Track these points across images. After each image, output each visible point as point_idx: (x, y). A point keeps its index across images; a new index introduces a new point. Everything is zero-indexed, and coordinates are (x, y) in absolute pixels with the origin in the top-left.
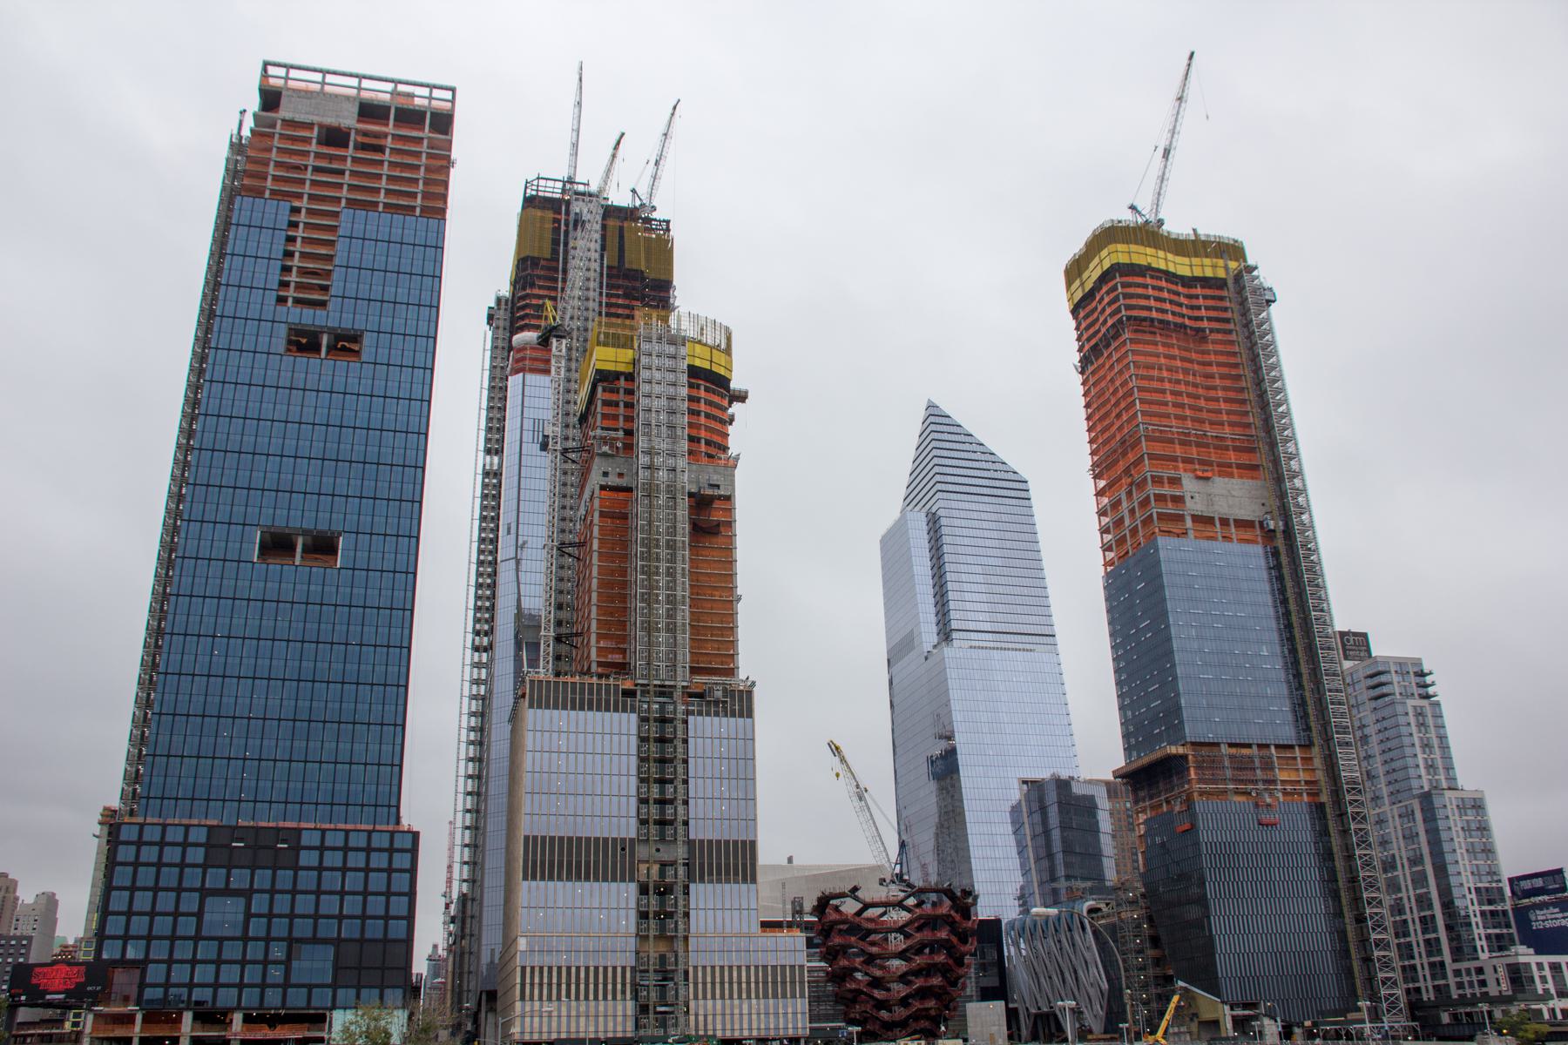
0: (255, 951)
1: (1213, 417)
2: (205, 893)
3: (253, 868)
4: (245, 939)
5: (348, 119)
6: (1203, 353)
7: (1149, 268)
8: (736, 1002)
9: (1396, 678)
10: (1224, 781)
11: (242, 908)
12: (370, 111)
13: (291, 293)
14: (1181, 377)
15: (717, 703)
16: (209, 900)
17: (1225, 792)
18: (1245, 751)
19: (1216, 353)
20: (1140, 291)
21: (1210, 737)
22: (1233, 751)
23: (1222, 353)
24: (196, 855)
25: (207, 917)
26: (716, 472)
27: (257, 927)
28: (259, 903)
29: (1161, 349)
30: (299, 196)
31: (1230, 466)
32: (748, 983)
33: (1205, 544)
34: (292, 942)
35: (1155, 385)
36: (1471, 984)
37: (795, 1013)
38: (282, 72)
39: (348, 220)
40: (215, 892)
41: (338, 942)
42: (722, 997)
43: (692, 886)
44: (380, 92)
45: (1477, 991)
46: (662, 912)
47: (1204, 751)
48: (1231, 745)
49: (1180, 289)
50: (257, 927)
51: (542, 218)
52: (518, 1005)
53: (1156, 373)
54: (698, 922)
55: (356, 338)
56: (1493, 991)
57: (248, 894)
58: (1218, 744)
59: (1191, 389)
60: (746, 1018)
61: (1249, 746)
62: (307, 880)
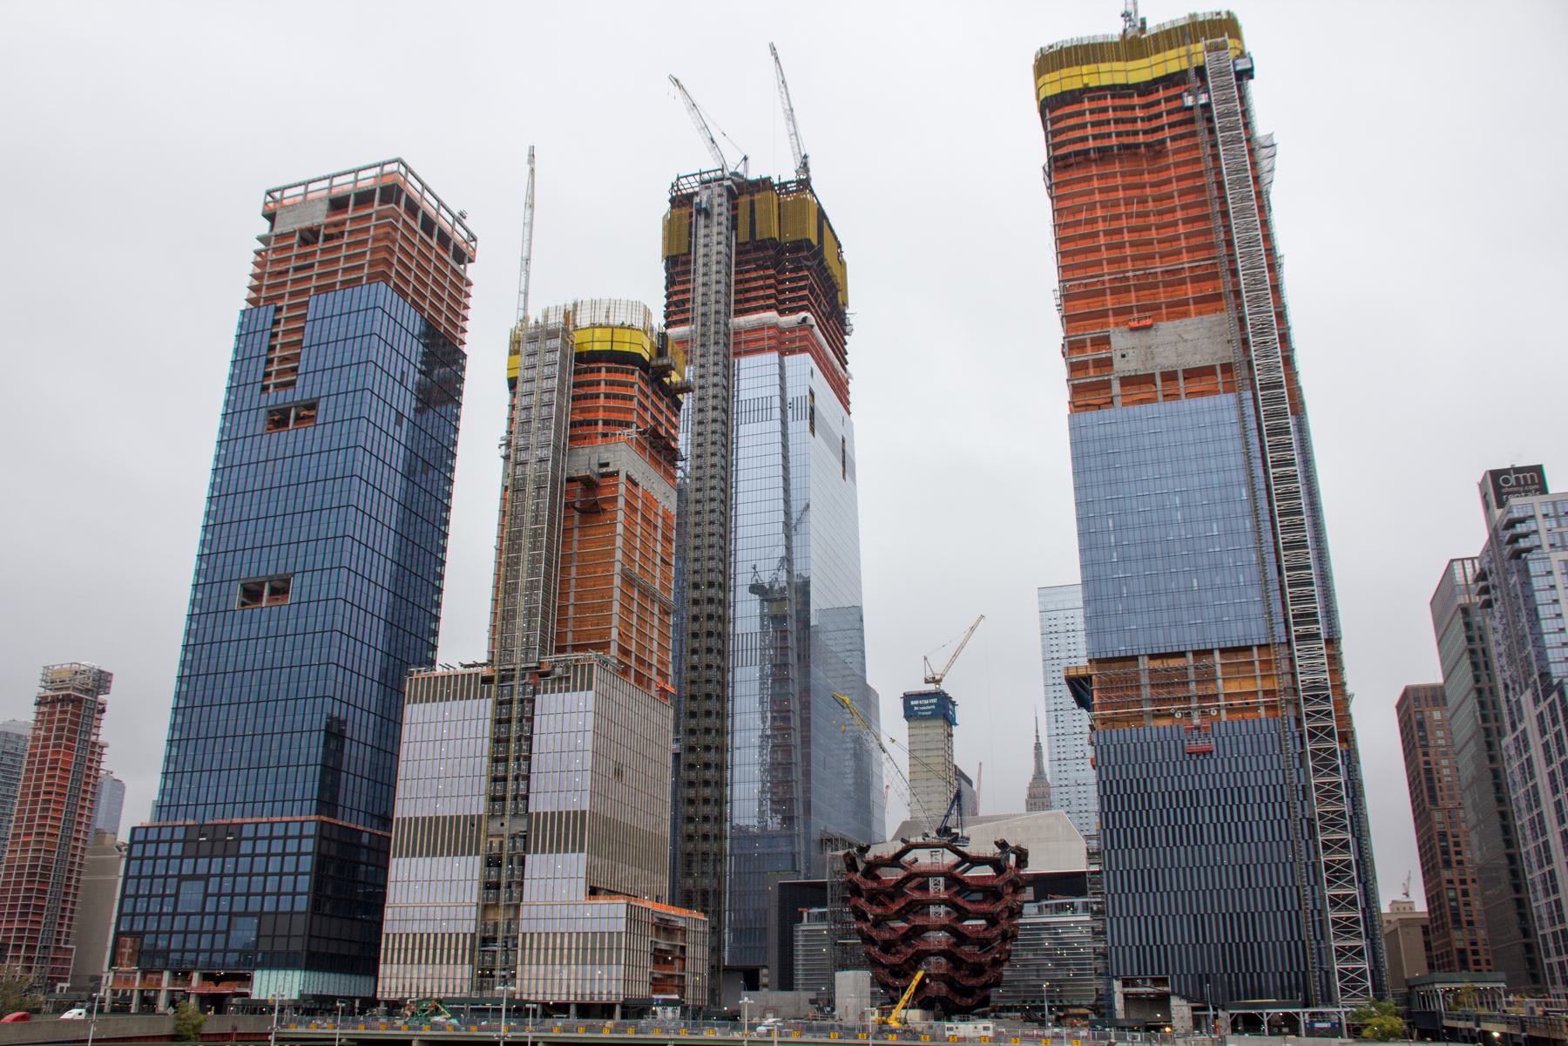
1: (1167, 247)
2: (181, 878)
3: (211, 857)
4: (203, 913)
5: (319, 216)
6: (1159, 170)
7: (1086, 90)
8: (557, 967)
9: (1543, 525)
10: (1139, 703)
12: (338, 204)
13: (273, 380)
14: (1123, 209)
15: (560, 679)
17: (1140, 716)
18: (1173, 663)
19: (1177, 165)
20: (1071, 122)
21: (1123, 650)
22: (1157, 664)
23: (1186, 163)
24: (177, 849)
26: (607, 451)
27: (210, 907)
28: (213, 886)
29: (1096, 184)
30: (282, 297)
31: (1186, 303)
32: (570, 949)
33: (1137, 410)
35: (1082, 230)
37: (609, 980)
39: (317, 305)
41: (261, 914)
42: (546, 963)
43: (528, 858)
44: (344, 185)
46: (501, 884)
47: (1115, 670)
48: (1152, 657)
49: (1136, 100)
51: (680, 217)
52: (381, 967)
53: (1083, 216)
54: (531, 890)
55: (312, 406)
57: (206, 878)
58: (1135, 658)
59: (1134, 222)
60: (565, 983)
61: (1182, 654)
62: (244, 864)
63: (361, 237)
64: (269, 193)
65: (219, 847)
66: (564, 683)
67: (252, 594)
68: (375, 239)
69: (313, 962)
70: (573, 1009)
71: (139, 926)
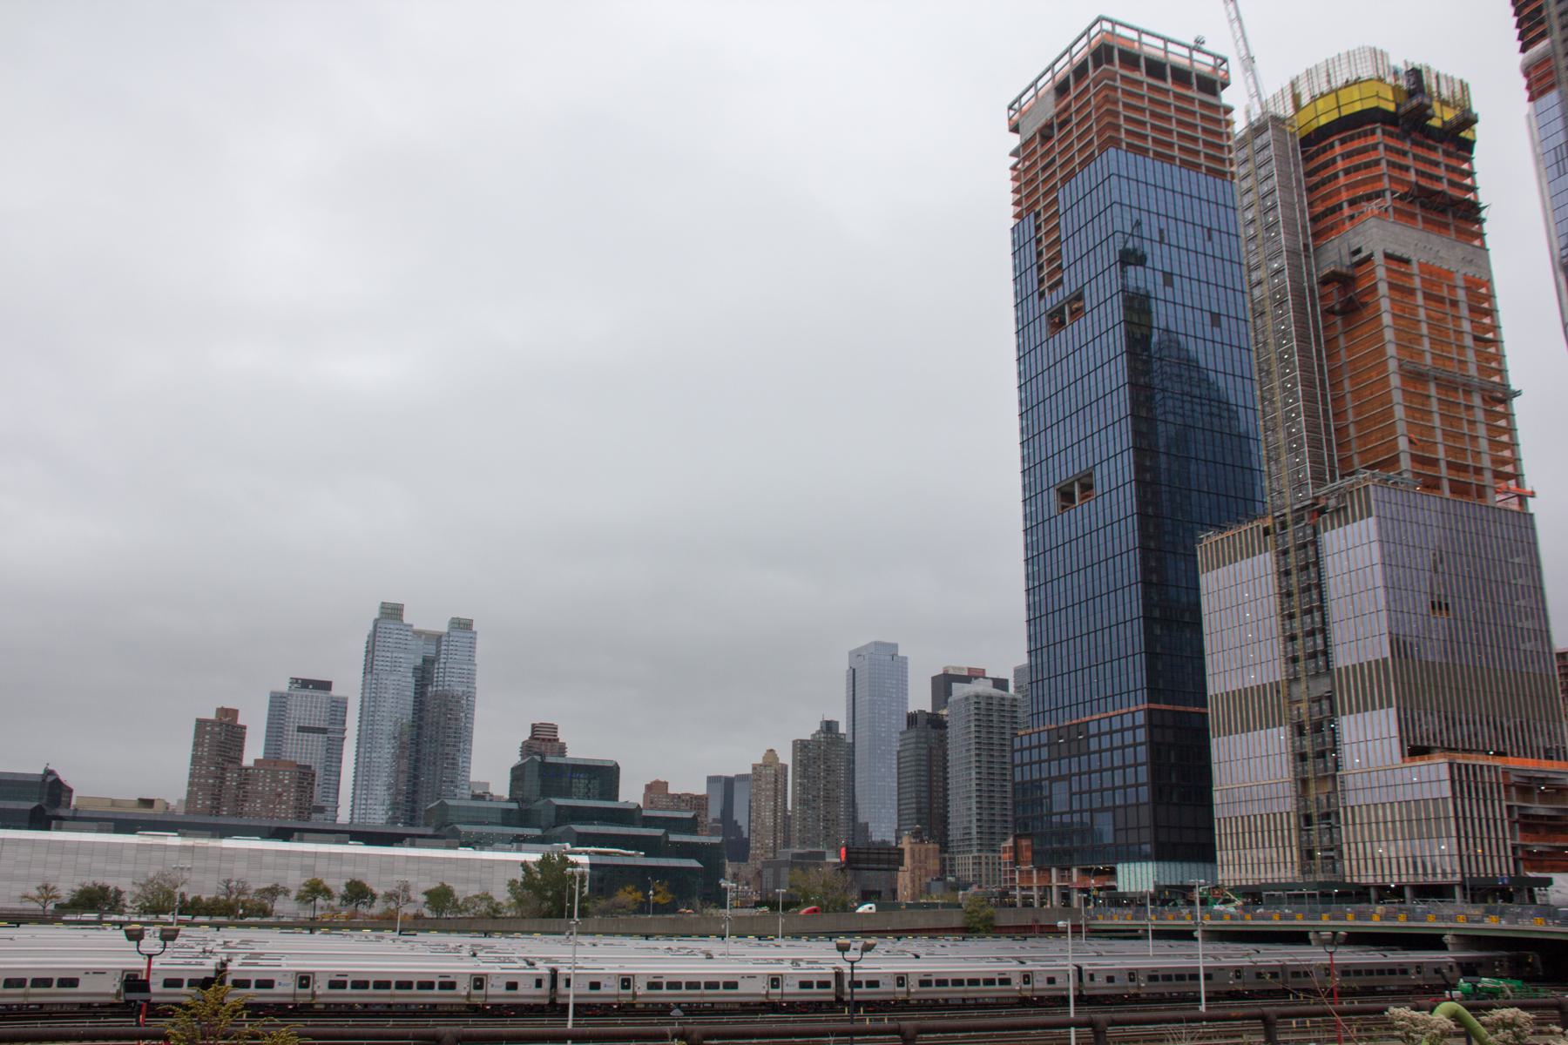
3: (1070, 758)
4: (1071, 812)
5: (1049, 110)
12: (1061, 89)
13: (1047, 284)
26: (1357, 234)
27: (1076, 806)
30: (1037, 202)
41: (1114, 808)
46: (1317, 753)
55: (1079, 297)
63: (1085, 112)
64: (1010, 108)
65: (1074, 746)
66: (1341, 514)
67: (1066, 496)
68: (1098, 108)
69: (1162, 853)
70: (1408, 893)
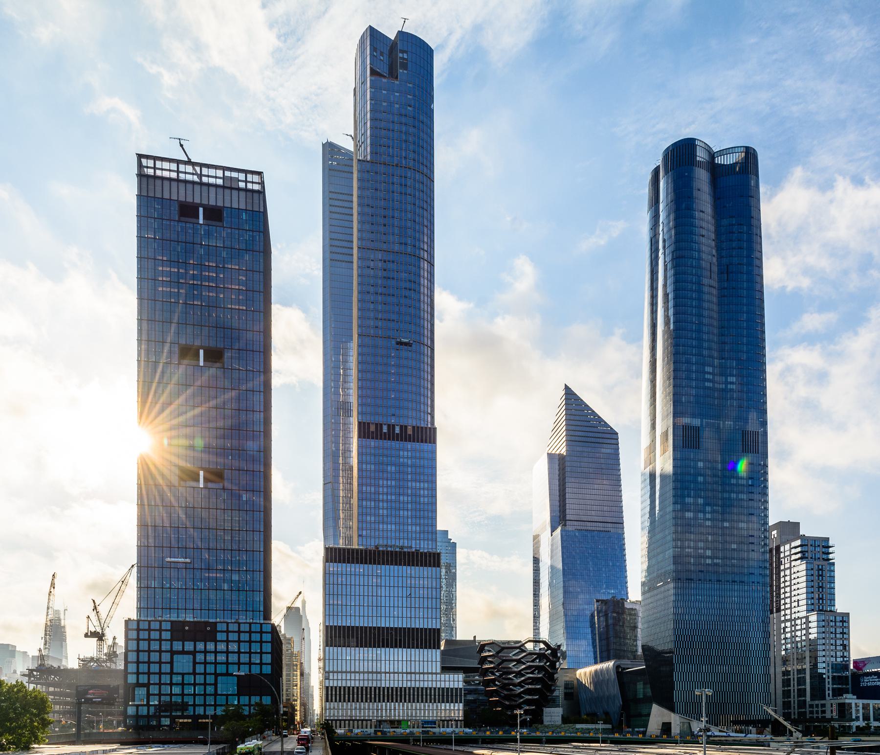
0: (200, 679)
11: (192, 660)
16: (175, 656)
24: (167, 635)
25: (175, 664)
27: (200, 669)
28: (200, 657)
34: (216, 675)
36: (817, 712)
38: (151, 163)
40: (178, 653)
45: (820, 716)
50: (200, 669)
56: (828, 715)
71: (143, 679)
